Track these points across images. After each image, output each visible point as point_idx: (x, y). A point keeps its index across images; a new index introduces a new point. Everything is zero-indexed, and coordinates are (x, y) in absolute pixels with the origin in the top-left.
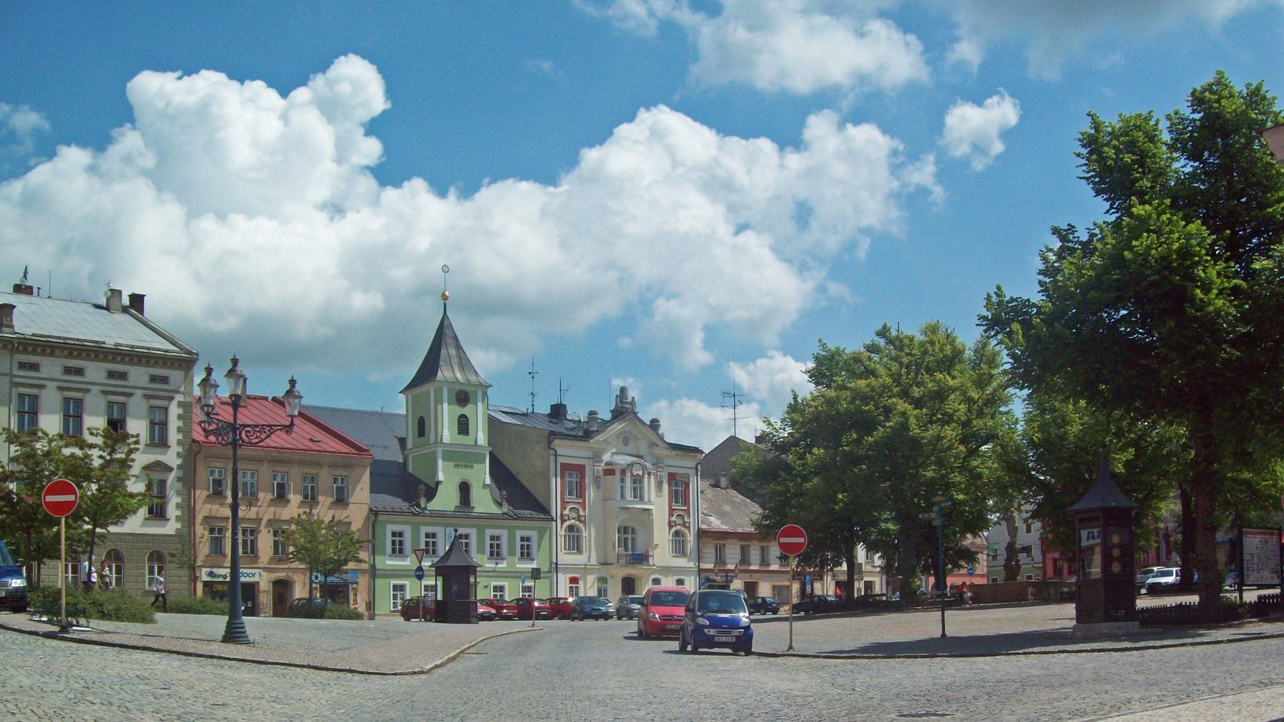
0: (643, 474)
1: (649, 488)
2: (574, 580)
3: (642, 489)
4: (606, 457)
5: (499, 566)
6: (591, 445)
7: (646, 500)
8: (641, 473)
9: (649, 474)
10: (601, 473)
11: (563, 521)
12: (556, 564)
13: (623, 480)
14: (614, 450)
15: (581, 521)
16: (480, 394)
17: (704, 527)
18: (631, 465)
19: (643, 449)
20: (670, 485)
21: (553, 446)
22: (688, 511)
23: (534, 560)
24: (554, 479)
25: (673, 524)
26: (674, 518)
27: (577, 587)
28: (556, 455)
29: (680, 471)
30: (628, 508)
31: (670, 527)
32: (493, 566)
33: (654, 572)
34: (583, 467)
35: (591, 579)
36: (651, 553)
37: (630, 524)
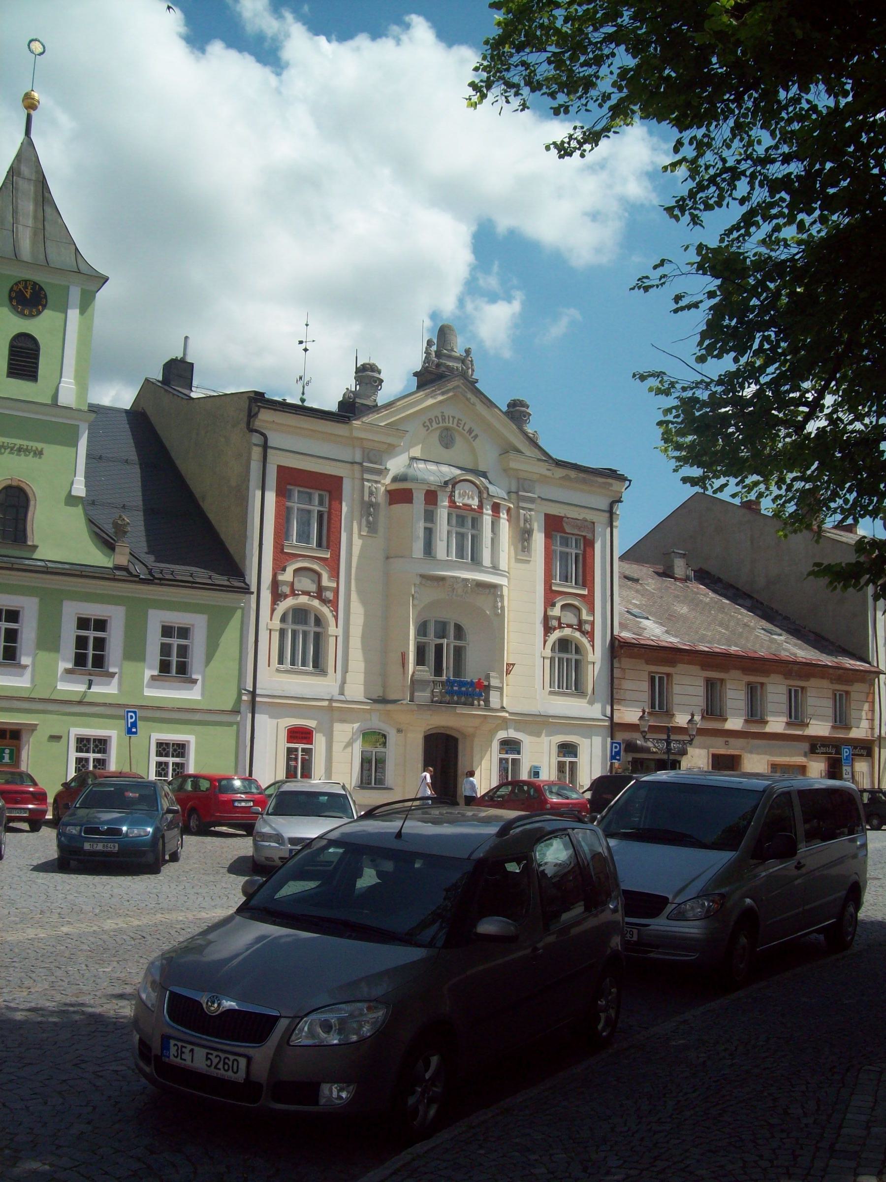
0: (481, 506)
1: (494, 541)
2: (299, 735)
3: (476, 541)
4: (396, 465)
5: (95, 689)
6: (356, 434)
7: (487, 561)
8: (474, 503)
9: (496, 508)
10: (381, 497)
11: (277, 596)
12: (253, 694)
13: (430, 516)
14: (416, 452)
15: (324, 601)
16: (75, 294)
17: (626, 635)
18: (454, 483)
19: (487, 458)
20: (548, 536)
21: (257, 424)
22: (589, 600)
23: (195, 682)
24: (258, 493)
25: (555, 623)
26: (556, 611)
28: (265, 447)
29: (572, 513)
30: (443, 579)
31: (548, 630)
32: (81, 688)
33: (505, 724)
34: (340, 479)
35: (344, 731)
36: (494, 682)
37: (451, 616)
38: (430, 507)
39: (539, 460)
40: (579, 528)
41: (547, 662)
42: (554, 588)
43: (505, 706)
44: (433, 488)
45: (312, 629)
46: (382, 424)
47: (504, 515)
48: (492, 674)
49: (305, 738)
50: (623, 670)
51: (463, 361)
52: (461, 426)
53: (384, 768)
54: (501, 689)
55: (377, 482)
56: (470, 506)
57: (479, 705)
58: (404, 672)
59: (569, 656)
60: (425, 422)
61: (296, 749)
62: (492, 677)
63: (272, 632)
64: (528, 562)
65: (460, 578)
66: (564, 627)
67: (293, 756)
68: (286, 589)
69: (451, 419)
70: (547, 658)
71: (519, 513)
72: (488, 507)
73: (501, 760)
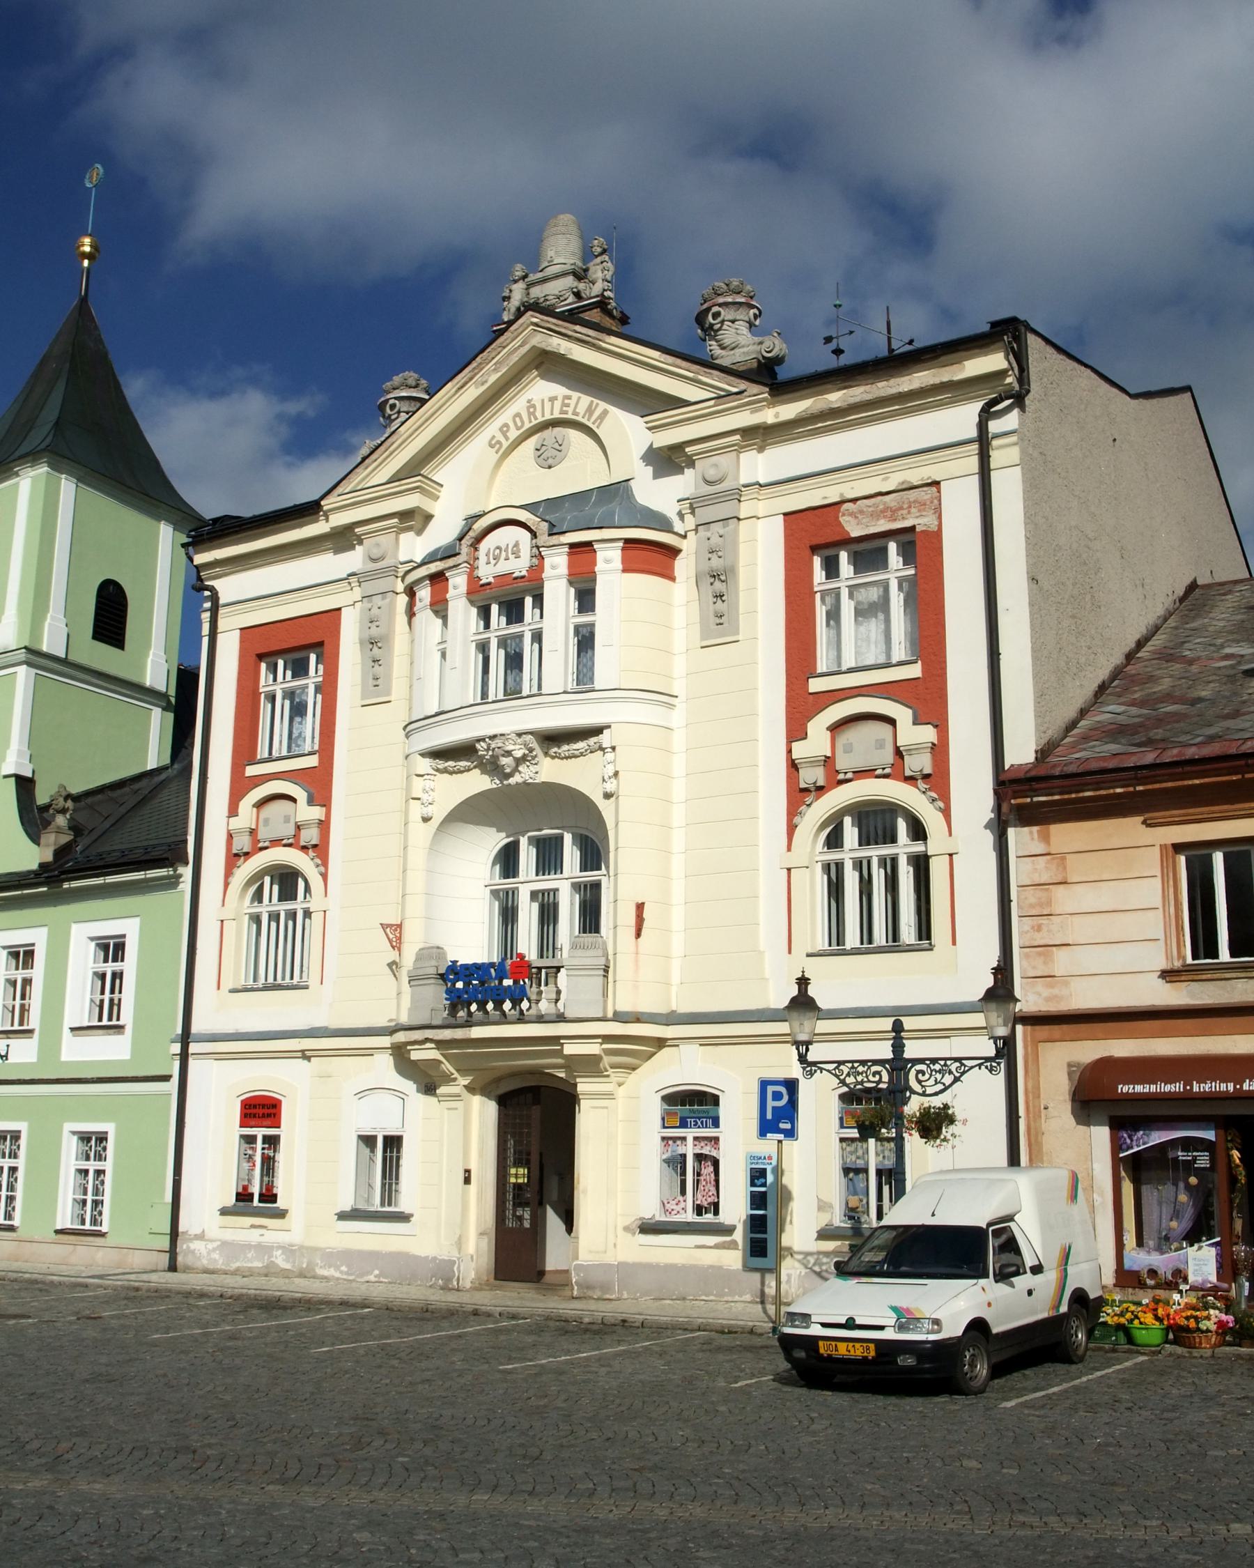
26: (817, 741)
27: (272, 1141)
49: (269, 1115)
59: (886, 850)
69: (548, 405)
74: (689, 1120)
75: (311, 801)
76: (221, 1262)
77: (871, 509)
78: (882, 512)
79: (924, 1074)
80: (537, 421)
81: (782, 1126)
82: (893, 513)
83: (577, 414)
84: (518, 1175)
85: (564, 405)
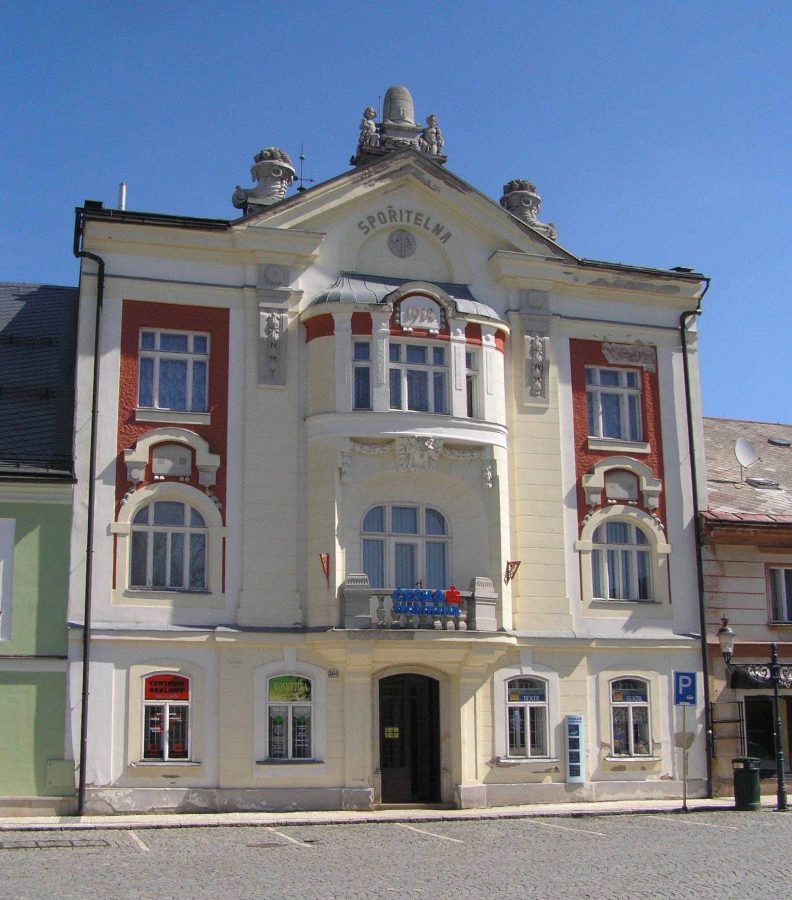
0: (446, 330)
8: (434, 326)
9: (474, 332)
12: (86, 629)
13: (363, 351)
25: (596, 499)
26: (596, 480)
31: (584, 509)
34: (224, 313)
38: (362, 338)
39: (547, 259)
40: (631, 356)
41: (588, 559)
42: (591, 447)
43: (505, 626)
44: (362, 310)
45: (187, 530)
46: (285, 226)
47: (489, 341)
48: (479, 579)
49: (177, 691)
50: (721, 563)
51: (424, 134)
52: (423, 223)
53: (308, 731)
54: (497, 603)
55: (281, 311)
56: (428, 331)
57: (457, 628)
58: (328, 587)
59: (626, 547)
60: (362, 222)
61: (161, 709)
62: (482, 584)
63: (118, 538)
64: (542, 411)
65: (413, 437)
66: (612, 504)
67: (156, 719)
68: (139, 475)
69: (405, 215)
70: (586, 552)
71: (522, 340)
72: (459, 330)
73: (511, 711)
74: (525, 697)
75: (212, 451)
76: (134, 805)
77: (619, 350)
78: (625, 353)
79: (786, 671)
80: (401, 223)
81: (688, 698)
82: (631, 356)
83: (428, 229)
84: (393, 733)
85: (417, 219)
